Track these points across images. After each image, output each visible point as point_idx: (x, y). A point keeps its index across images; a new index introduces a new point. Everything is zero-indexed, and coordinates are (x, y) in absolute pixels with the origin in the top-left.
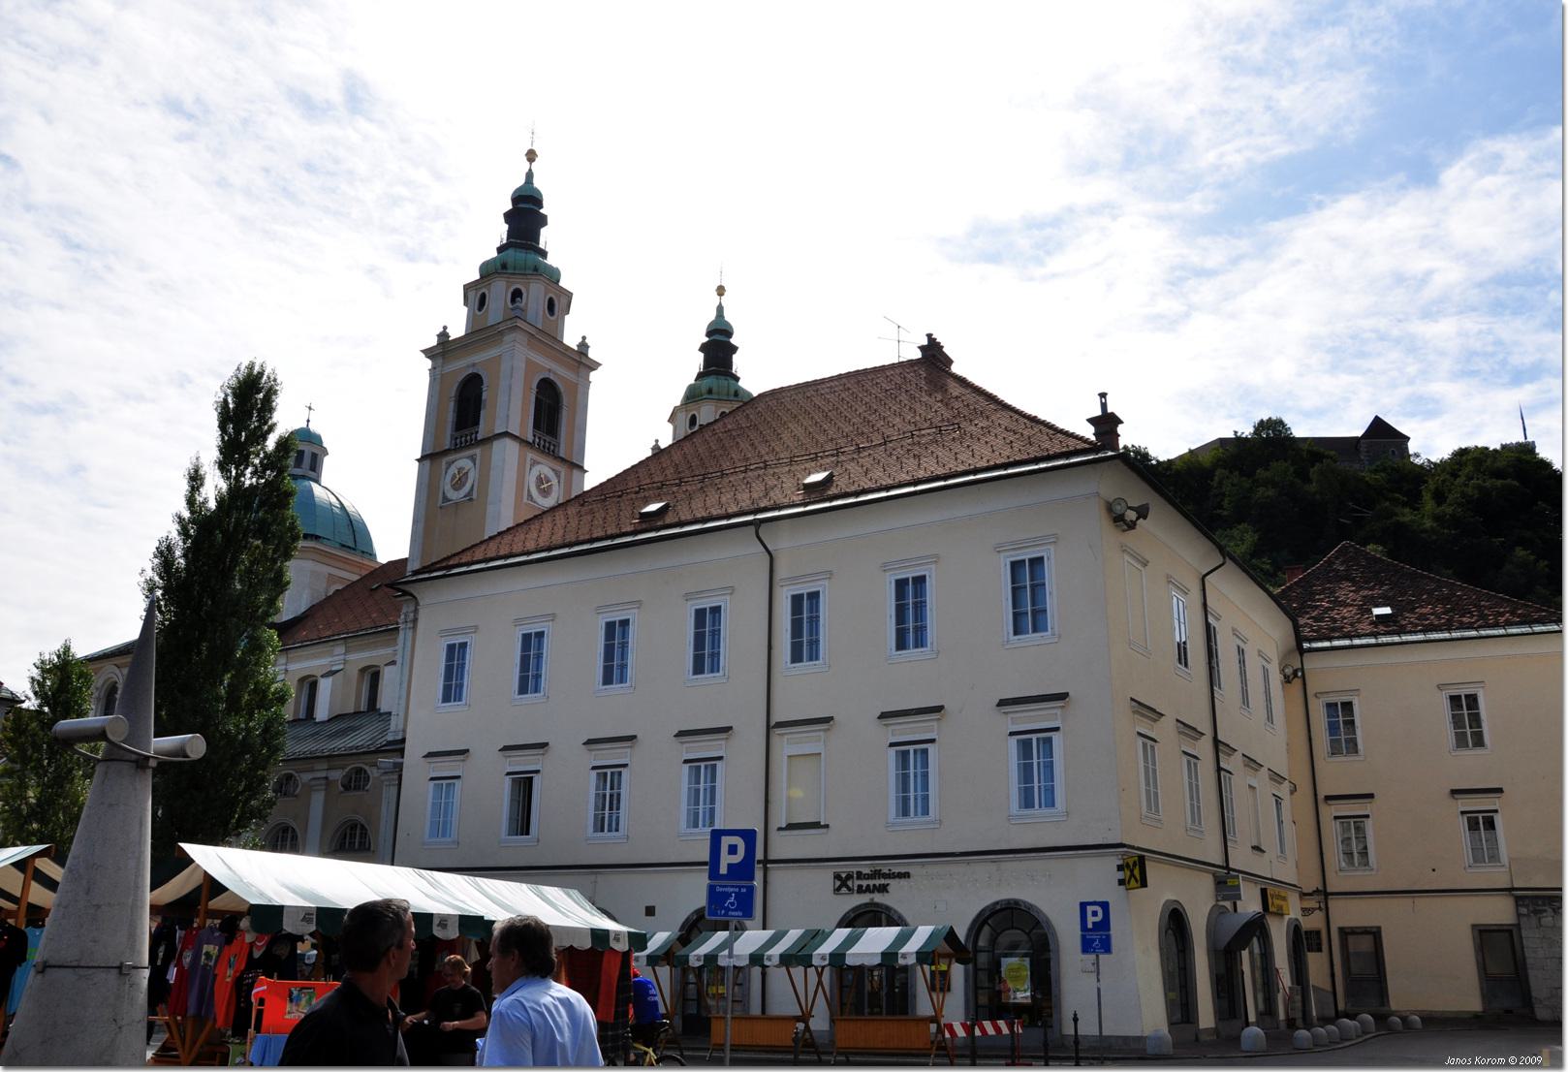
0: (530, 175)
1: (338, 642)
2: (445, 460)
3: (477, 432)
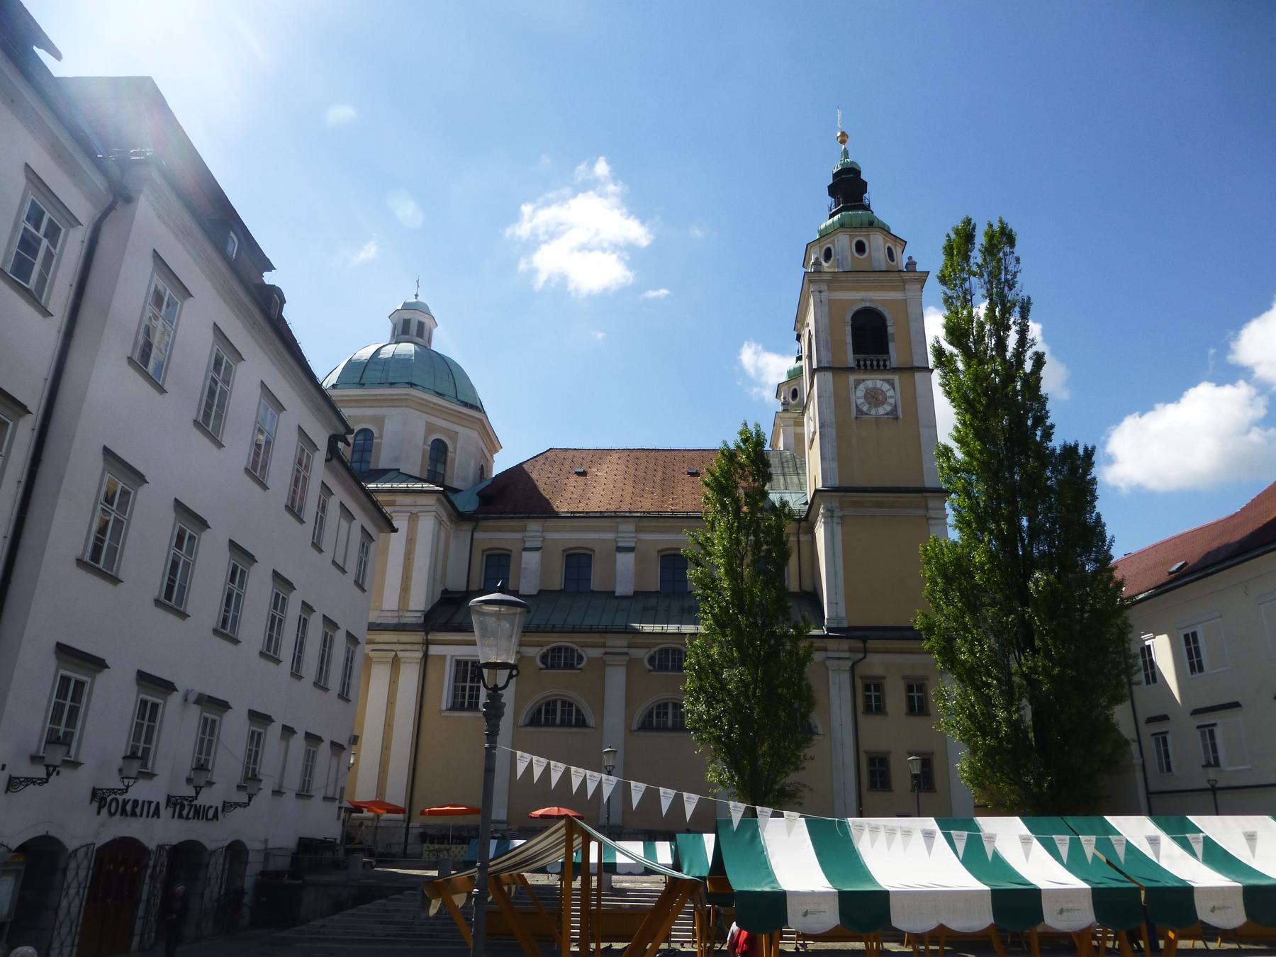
0: (846, 153)
1: (631, 520)
2: (852, 378)
3: (885, 361)
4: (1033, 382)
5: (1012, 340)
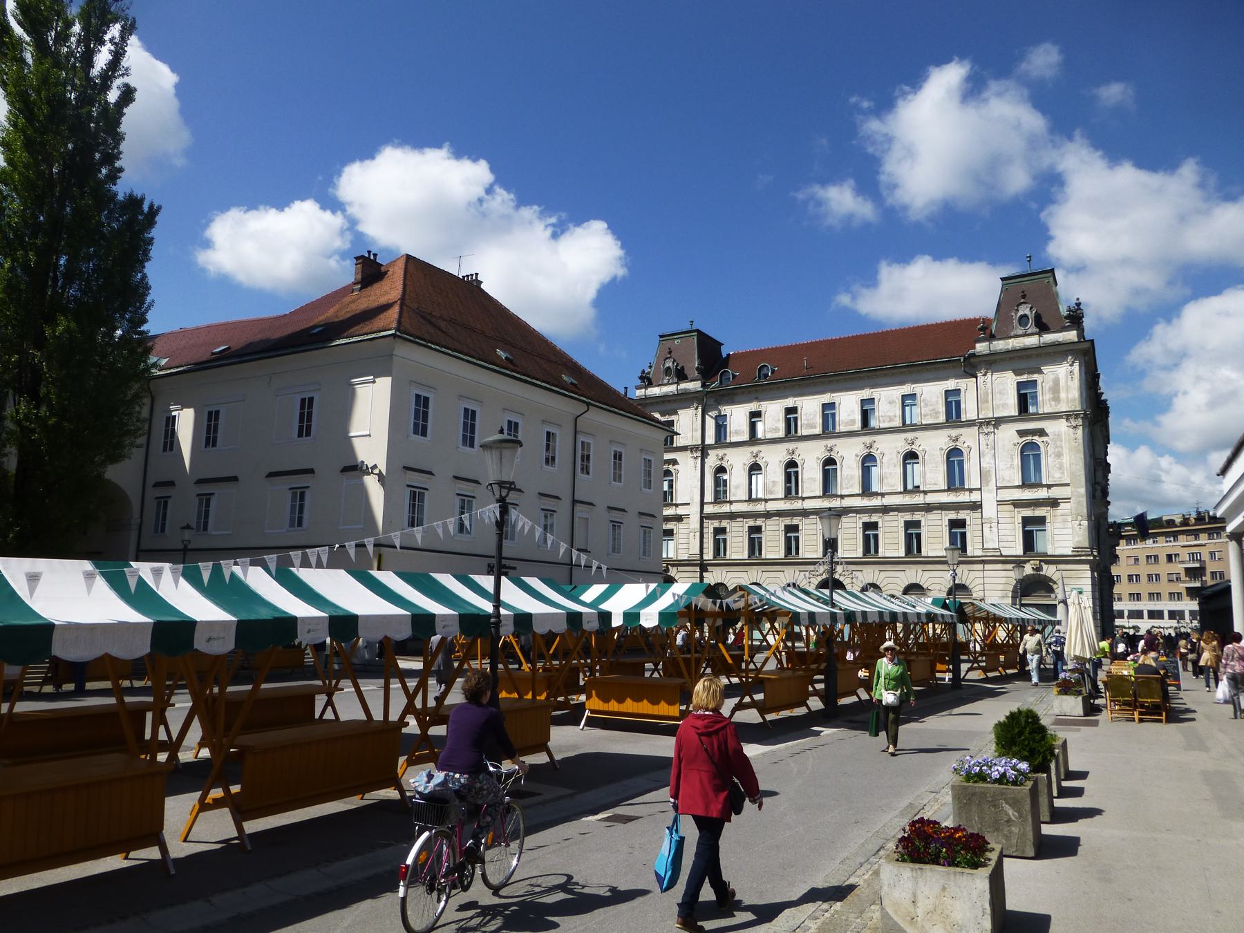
4: (113, 116)
5: (102, 58)
